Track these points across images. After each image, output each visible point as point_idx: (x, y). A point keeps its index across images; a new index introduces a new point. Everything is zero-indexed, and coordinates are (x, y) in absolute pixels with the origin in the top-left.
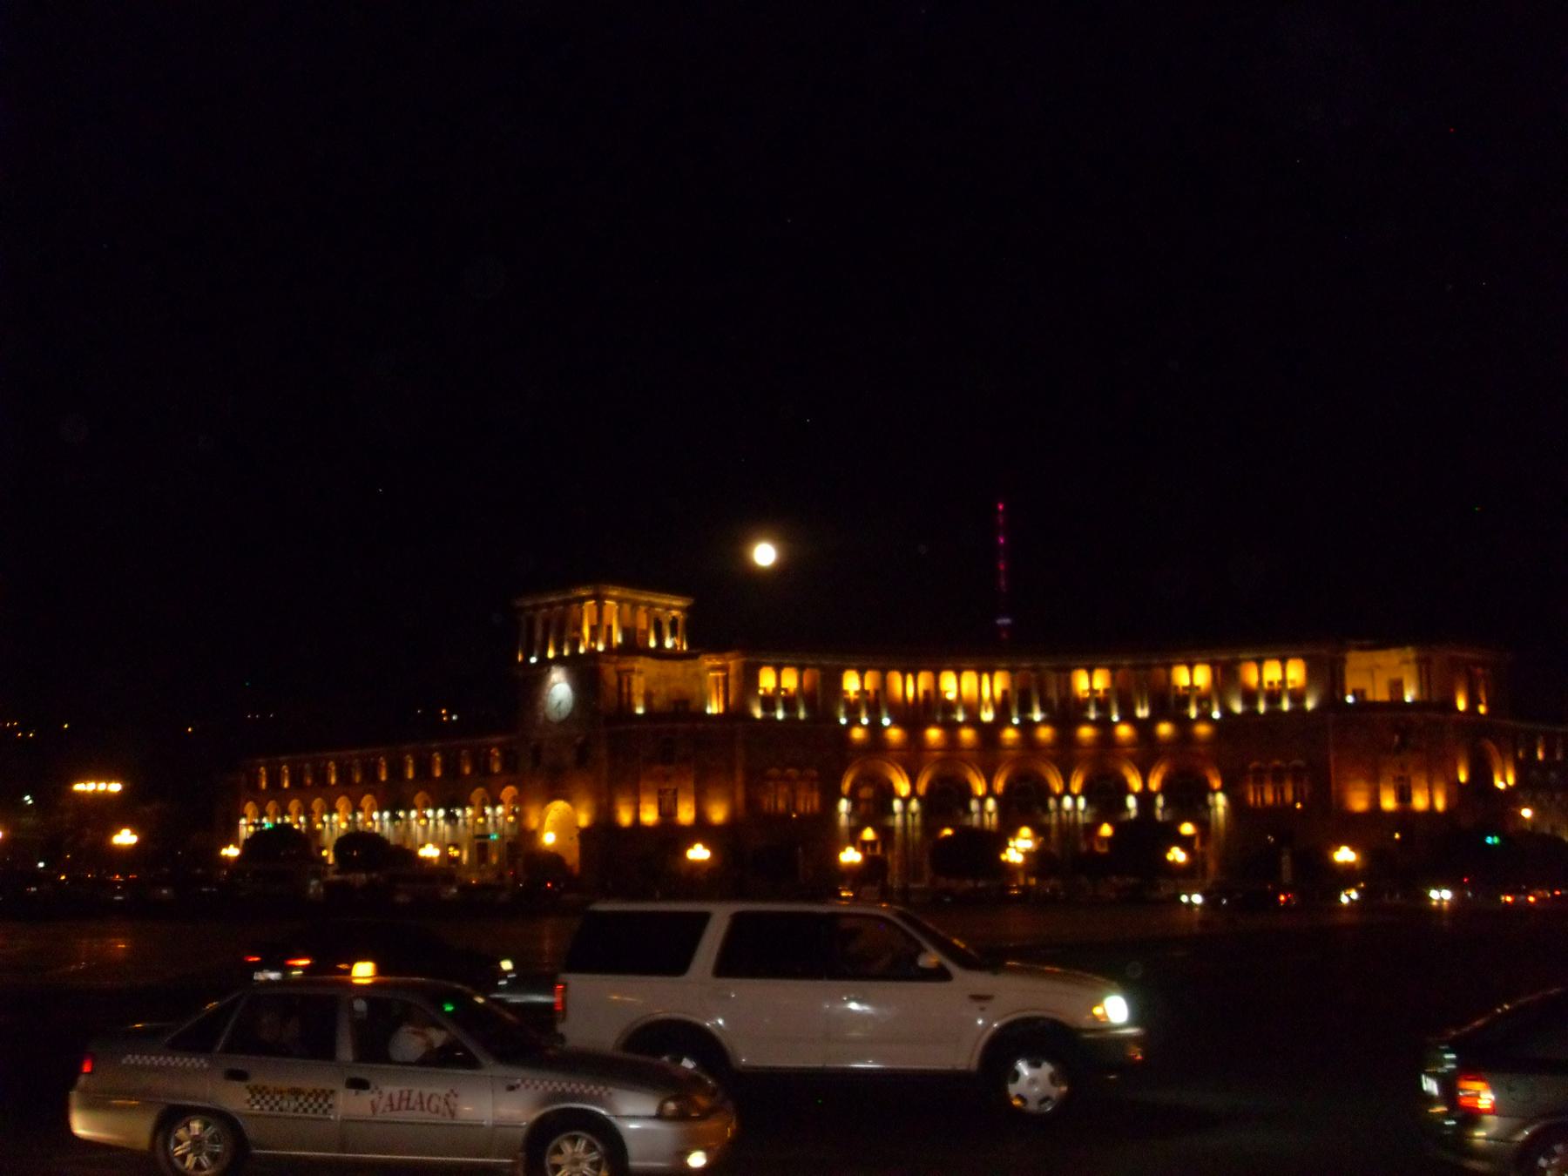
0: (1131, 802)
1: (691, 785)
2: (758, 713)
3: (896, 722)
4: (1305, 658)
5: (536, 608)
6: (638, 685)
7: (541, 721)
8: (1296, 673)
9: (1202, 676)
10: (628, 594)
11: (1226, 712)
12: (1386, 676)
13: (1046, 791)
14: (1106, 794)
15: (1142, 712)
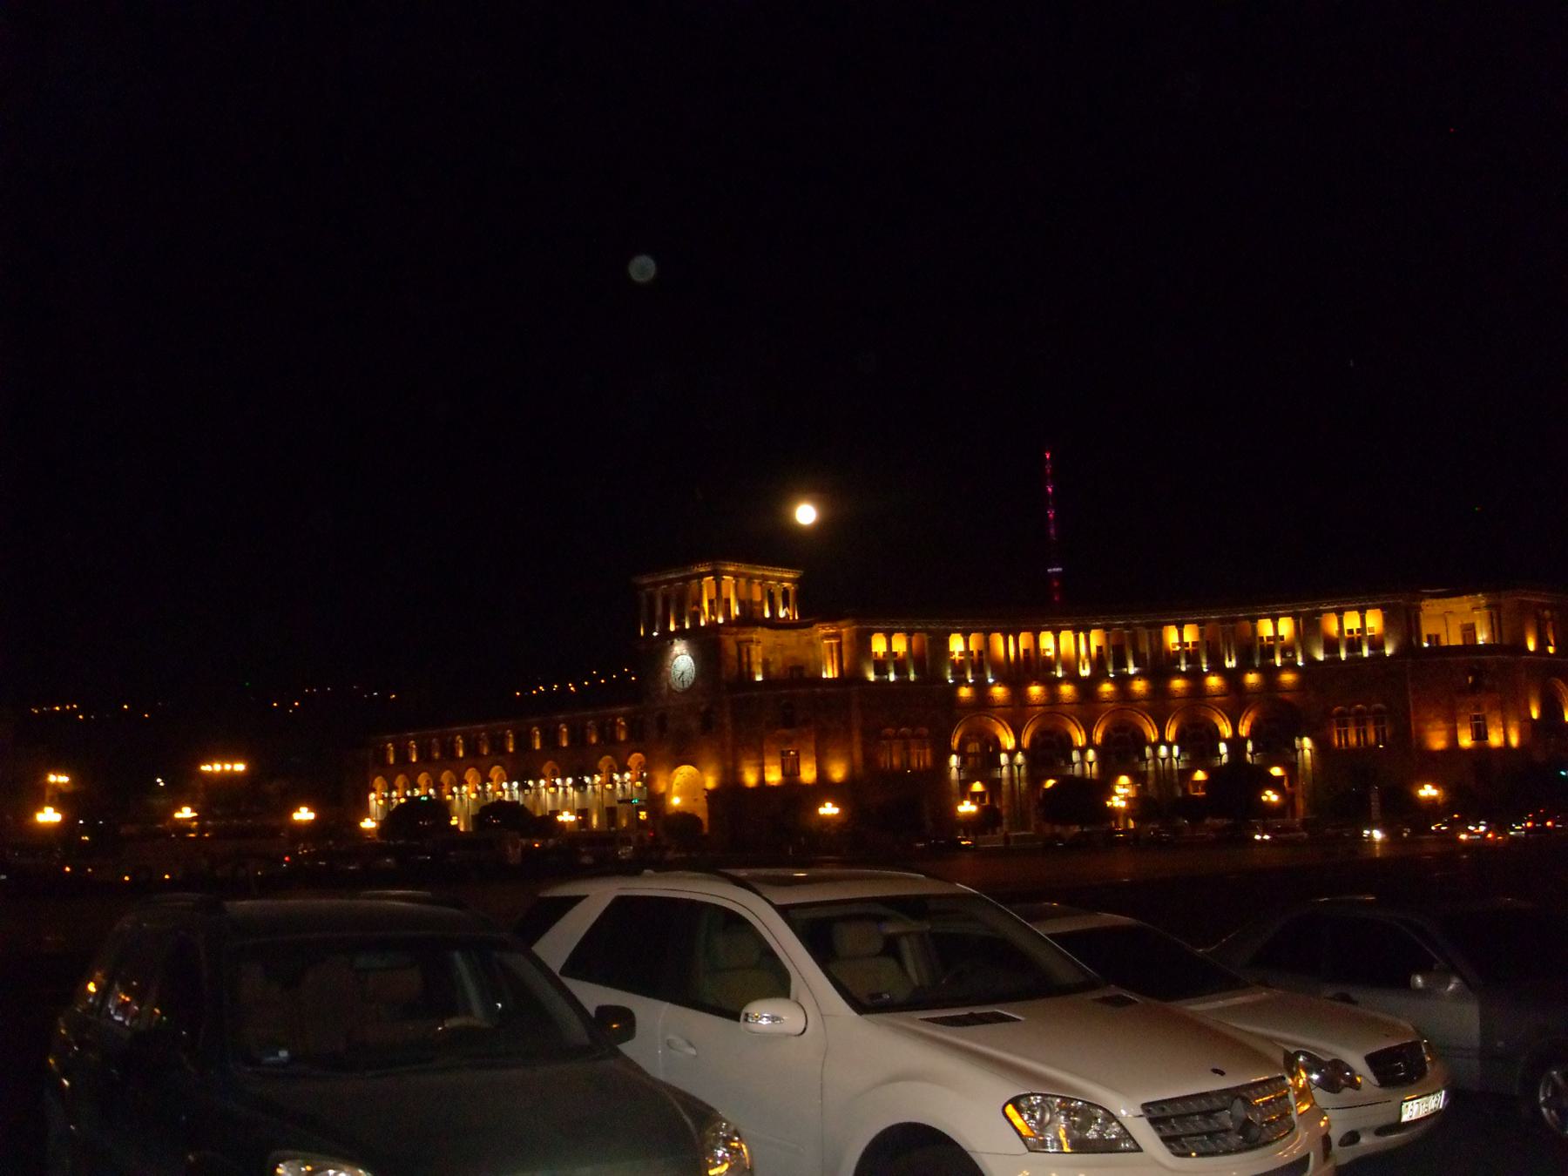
0: (1223, 748)
1: (812, 747)
2: (872, 677)
3: (1001, 680)
4: (1383, 608)
5: (656, 585)
6: (757, 654)
7: (665, 691)
8: (1374, 621)
9: (1286, 627)
10: (743, 568)
11: (1309, 659)
12: (1457, 621)
13: (1142, 740)
14: (1198, 741)
15: (1231, 664)
